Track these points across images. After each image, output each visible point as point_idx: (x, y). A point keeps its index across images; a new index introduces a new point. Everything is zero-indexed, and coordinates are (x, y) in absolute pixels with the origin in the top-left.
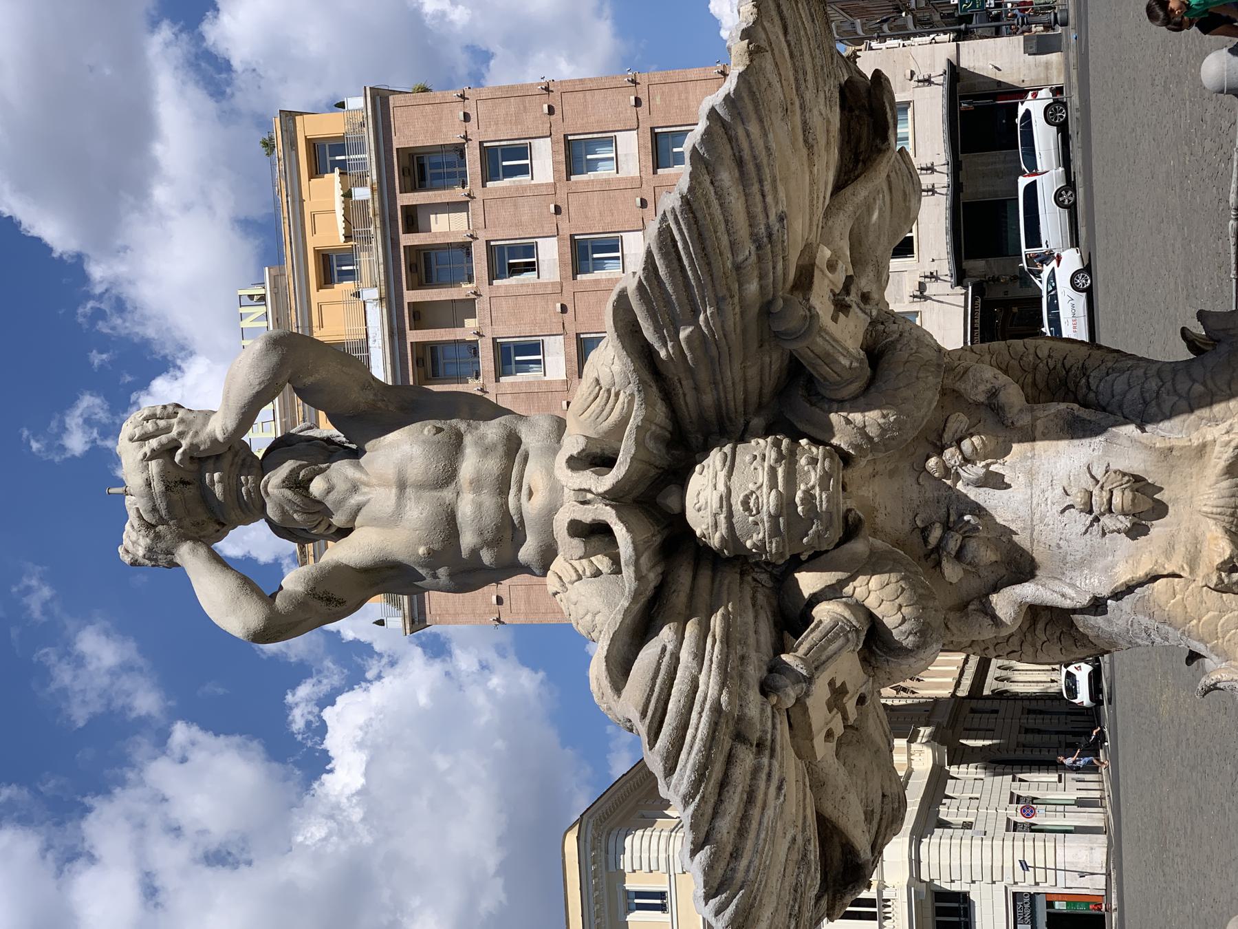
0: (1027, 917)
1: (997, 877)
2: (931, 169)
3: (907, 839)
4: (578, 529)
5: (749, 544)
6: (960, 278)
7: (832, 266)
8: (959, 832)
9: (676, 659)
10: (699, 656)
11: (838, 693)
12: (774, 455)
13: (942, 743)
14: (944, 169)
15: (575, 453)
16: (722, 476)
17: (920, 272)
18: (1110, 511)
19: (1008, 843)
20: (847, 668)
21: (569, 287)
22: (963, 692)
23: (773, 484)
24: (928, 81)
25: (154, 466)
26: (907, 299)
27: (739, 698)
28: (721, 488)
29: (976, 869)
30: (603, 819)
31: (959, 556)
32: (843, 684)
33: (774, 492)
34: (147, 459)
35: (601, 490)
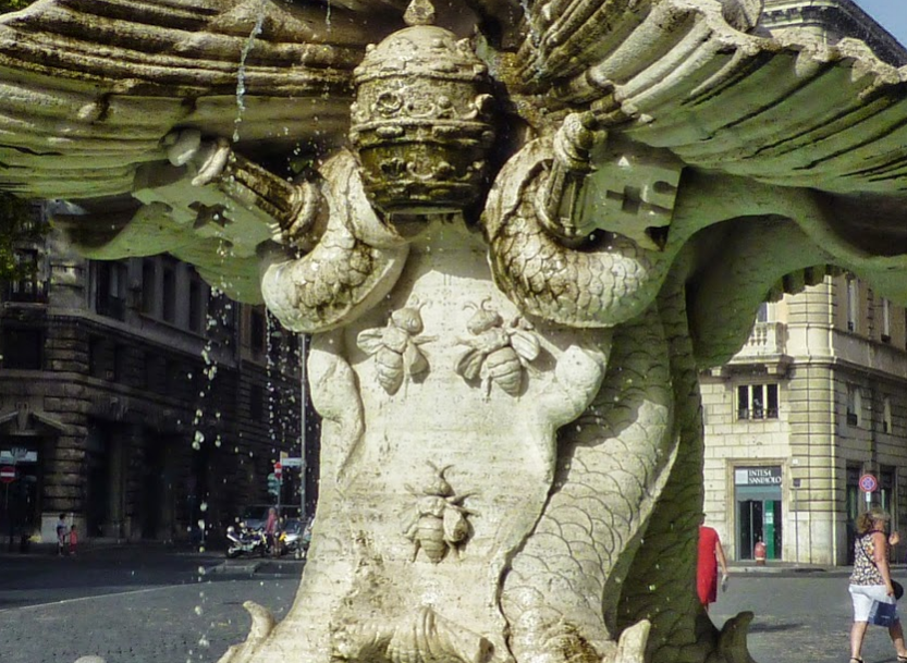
0: (756, 481)
7: (661, 187)
9: (192, 26)
12: (445, 129)
16: (426, 69)
18: (423, 515)
33: (400, 129)
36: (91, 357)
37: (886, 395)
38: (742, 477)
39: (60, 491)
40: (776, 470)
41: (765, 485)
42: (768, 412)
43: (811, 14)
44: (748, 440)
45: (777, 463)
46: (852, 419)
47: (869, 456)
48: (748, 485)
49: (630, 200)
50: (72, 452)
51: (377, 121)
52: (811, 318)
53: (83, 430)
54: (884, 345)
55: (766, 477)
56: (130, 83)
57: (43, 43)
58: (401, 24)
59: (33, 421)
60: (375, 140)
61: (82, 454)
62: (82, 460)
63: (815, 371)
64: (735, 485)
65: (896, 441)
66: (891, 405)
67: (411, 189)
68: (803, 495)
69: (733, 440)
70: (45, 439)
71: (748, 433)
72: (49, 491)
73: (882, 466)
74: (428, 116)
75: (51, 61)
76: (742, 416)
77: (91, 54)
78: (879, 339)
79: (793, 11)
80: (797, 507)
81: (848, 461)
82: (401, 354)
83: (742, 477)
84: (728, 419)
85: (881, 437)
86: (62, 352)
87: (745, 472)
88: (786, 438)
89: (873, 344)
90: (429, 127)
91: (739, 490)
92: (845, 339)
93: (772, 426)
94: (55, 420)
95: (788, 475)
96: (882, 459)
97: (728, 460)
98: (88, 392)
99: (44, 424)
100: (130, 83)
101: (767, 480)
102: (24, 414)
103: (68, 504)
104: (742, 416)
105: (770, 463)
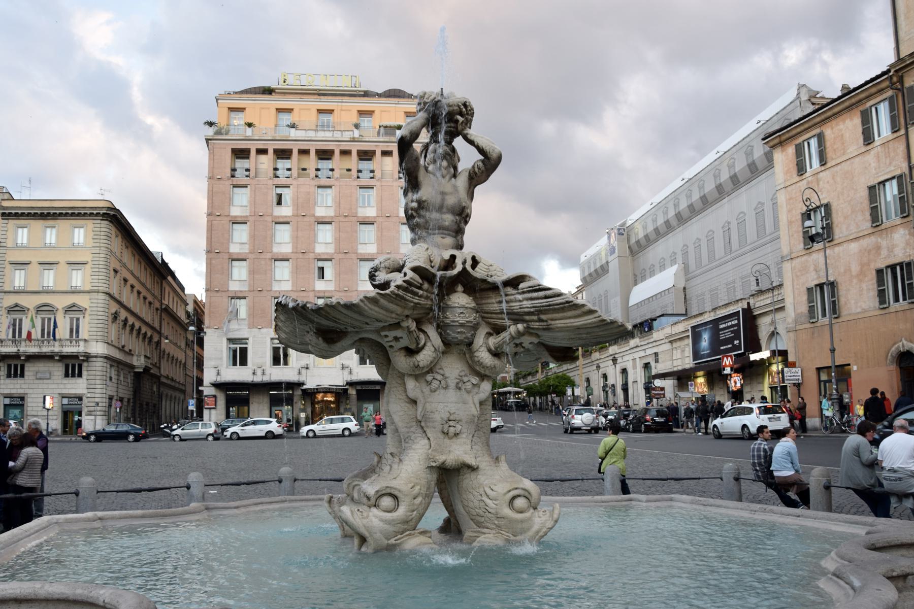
0: (71, 403)
3: (106, 353)
4: (453, 257)
5: (448, 313)
6: (351, 384)
8: (108, 376)
10: (421, 296)
11: (396, 339)
13: (145, 369)
15: (477, 258)
16: (469, 306)
18: (450, 426)
19: (104, 396)
20: (405, 342)
21: (354, 219)
22: (163, 380)
23: (467, 322)
25: (456, 108)
26: (342, 362)
28: (467, 306)
29: (93, 382)
31: (434, 378)
32: (399, 341)
34: (459, 106)
35: (467, 266)
37: (122, 369)
38: (65, 401)
40: (80, 399)
41: (75, 404)
42: (72, 374)
43: (106, 216)
44: (68, 386)
45: (81, 395)
46: (111, 378)
47: (115, 394)
48: (68, 404)
51: (458, 319)
52: (99, 337)
54: (122, 349)
55: (76, 401)
56: (412, 304)
57: (401, 293)
58: (456, 292)
60: (457, 324)
63: (99, 359)
64: (62, 405)
65: (124, 388)
66: (124, 374)
67: (465, 338)
68: (92, 409)
69: (61, 386)
71: (53, 383)
73: (120, 397)
74: (471, 319)
75: (403, 298)
76: (67, 375)
77: (409, 296)
78: (121, 347)
79: (99, 213)
80: (90, 413)
81: (109, 395)
82: (440, 381)
83: (65, 401)
84: (60, 377)
85: (120, 386)
87: (67, 399)
88: (85, 386)
89: (119, 348)
90: (471, 322)
91: (64, 407)
92: (110, 347)
93: (79, 380)
95: (85, 400)
96: (120, 395)
97: (59, 394)
100: (412, 304)
101: (76, 403)
104: (67, 375)
105: (78, 395)
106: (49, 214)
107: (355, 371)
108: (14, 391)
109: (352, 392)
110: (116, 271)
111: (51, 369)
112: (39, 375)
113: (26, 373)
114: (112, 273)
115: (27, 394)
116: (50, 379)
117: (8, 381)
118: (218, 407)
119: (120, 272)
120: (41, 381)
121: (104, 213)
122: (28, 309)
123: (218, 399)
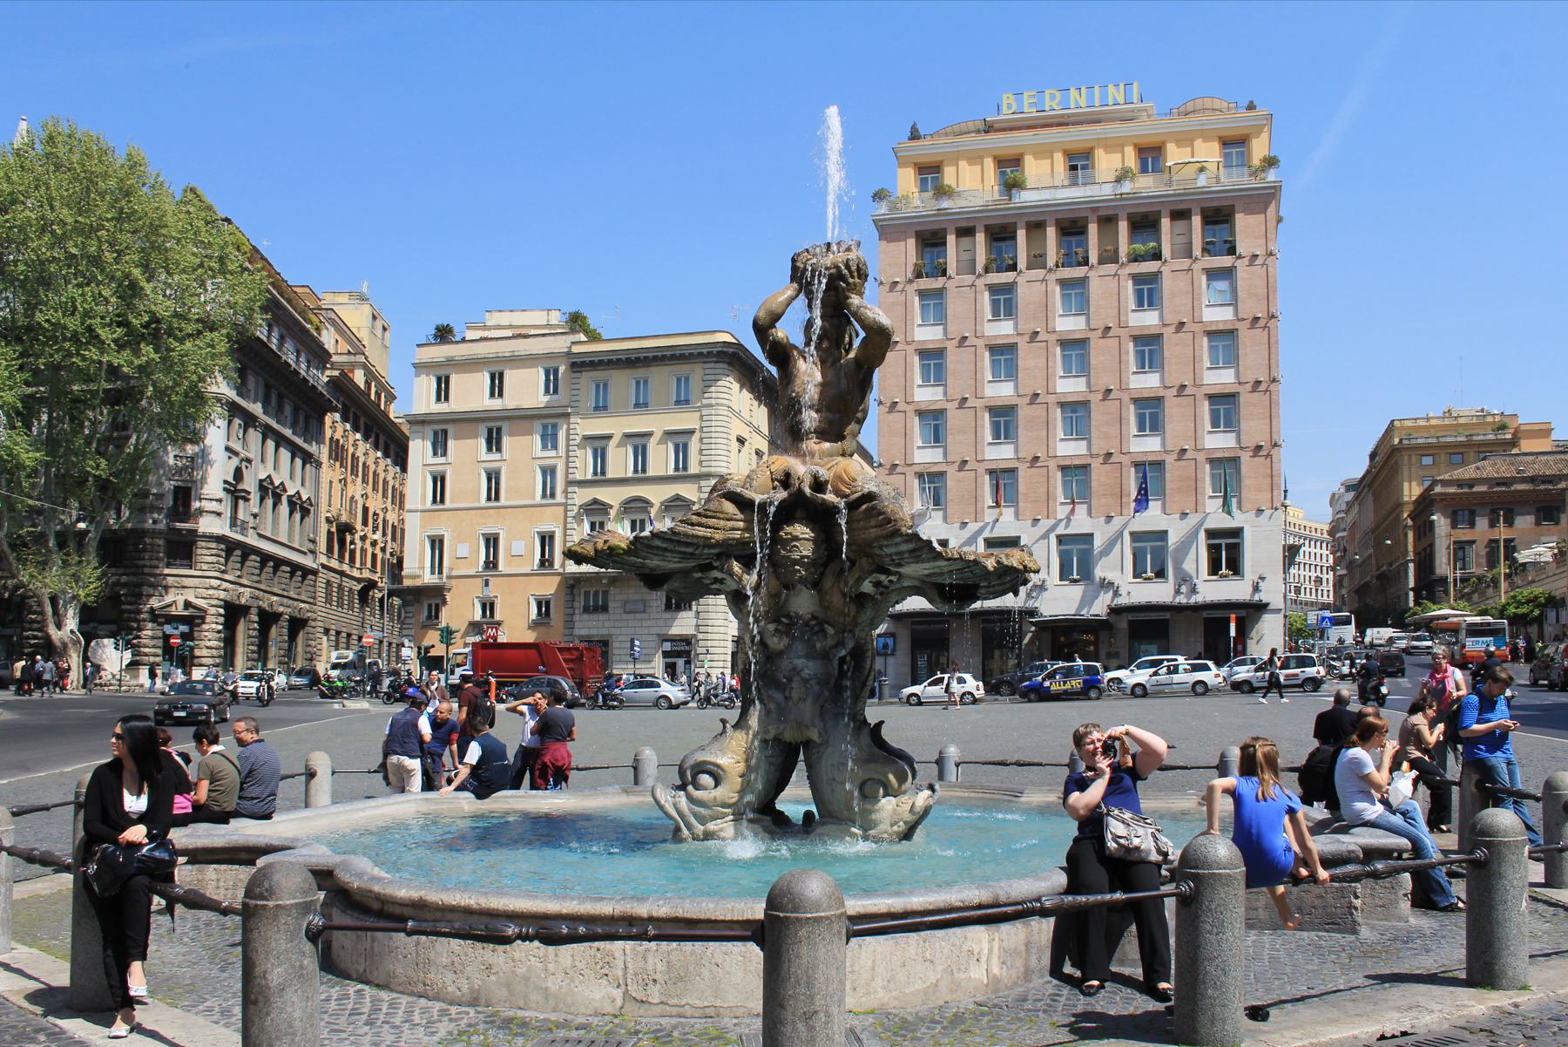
1: (702, 629)
2: (1194, 590)
6: (1115, 611)
11: (721, 581)
14: (1192, 601)
17: (1121, 584)
24: (1256, 589)
27: (712, 546)
30: (739, 359)
36: (227, 561)
39: (205, 652)
49: (877, 584)
50: (214, 626)
53: (222, 611)
59: (188, 605)
61: (220, 627)
62: (219, 632)
70: (193, 619)
72: (197, 652)
83: (667, 646)
86: (206, 555)
94: (201, 603)
97: (659, 635)
98: (226, 585)
99: (195, 607)
102: (181, 600)
103: (210, 661)
106: (638, 359)
107: (1123, 591)
108: (593, 632)
109: (1123, 623)
110: (741, 441)
111: (646, 597)
112: (629, 607)
113: (611, 604)
114: (736, 444)
115: (611, 635)
116: (644, 612)
117: (586, 616)
118: (898, 653)
119: (749, 440)
120: (632, 616)
121: (718, 352)
122: (611, 507)
123: (898, 640)
